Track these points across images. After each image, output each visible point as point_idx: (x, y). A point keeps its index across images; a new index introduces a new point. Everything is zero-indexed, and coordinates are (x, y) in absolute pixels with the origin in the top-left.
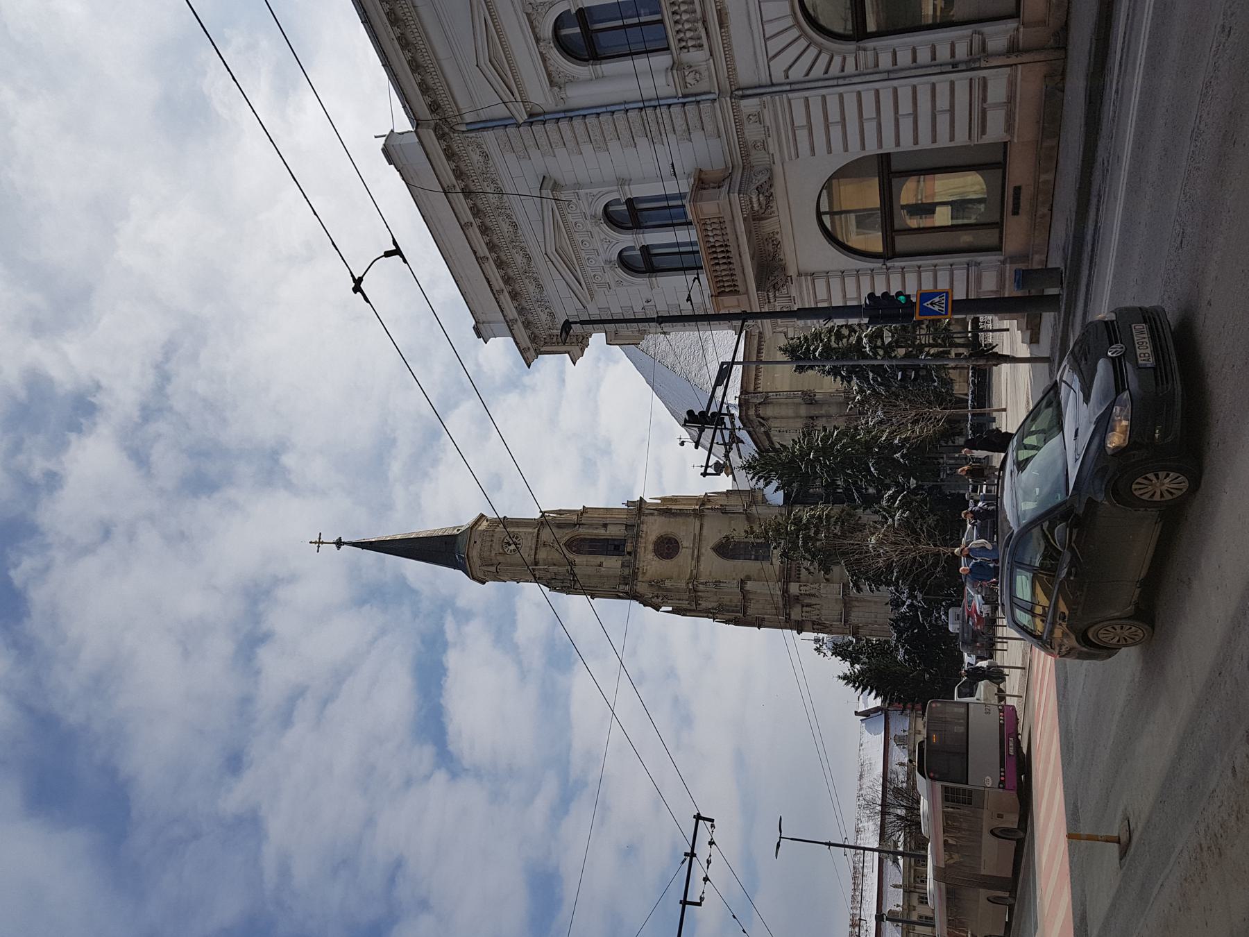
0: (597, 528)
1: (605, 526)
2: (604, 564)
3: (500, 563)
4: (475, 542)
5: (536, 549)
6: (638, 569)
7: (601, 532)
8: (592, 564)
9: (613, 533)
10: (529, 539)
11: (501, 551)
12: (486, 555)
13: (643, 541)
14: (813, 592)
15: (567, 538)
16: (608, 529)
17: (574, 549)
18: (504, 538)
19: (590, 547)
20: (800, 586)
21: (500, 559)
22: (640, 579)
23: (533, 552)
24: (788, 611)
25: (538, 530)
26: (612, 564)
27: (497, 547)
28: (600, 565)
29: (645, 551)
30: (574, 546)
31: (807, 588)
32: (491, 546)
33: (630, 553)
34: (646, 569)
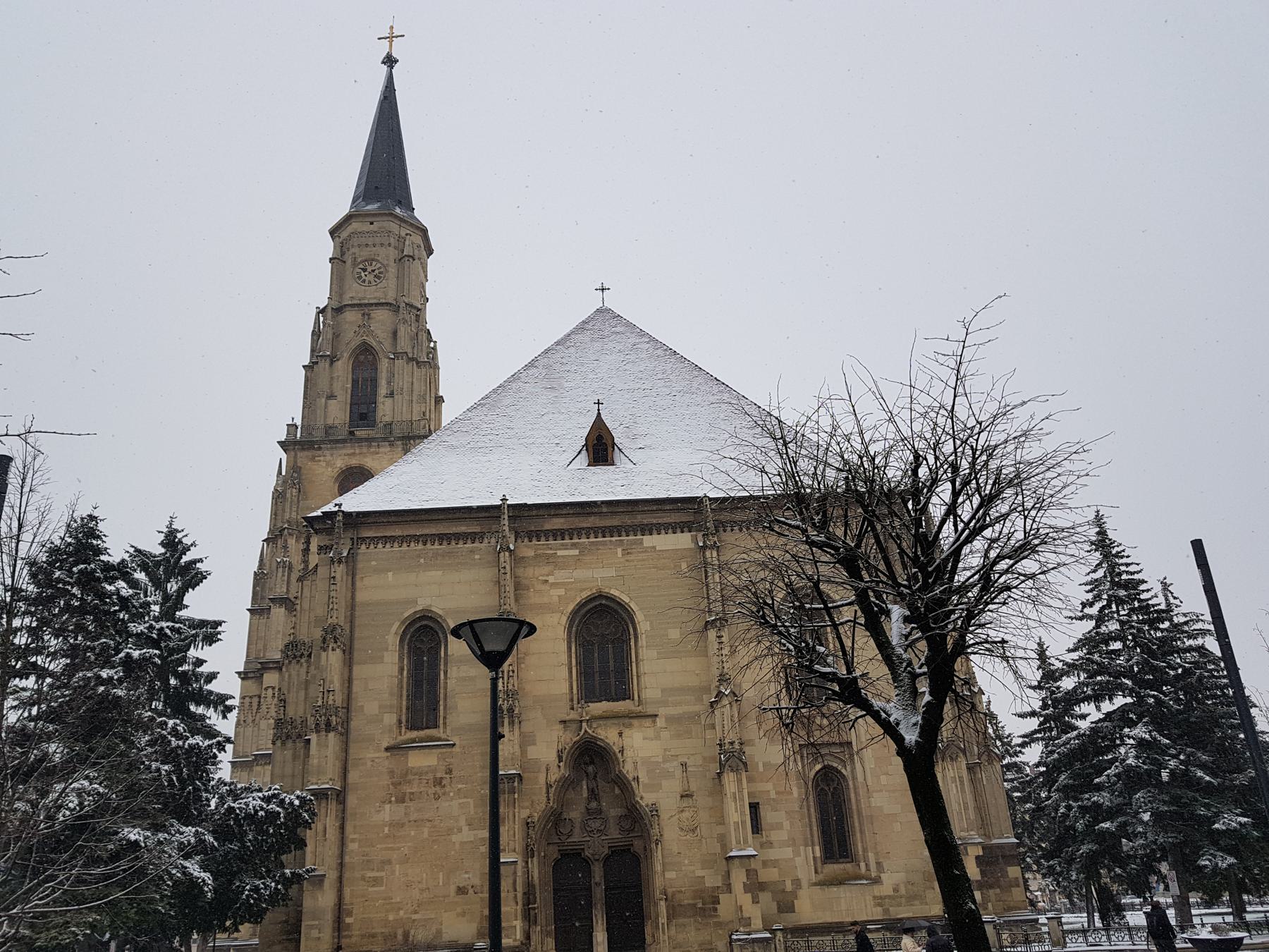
0: (389, 383)
1: (391, 395)
2: (330, 402)
3: (345, 262)
4: (372, 223)
5: (360, 305)
6: (320, 448)
7: (383, 390)
8: (335, 385)
9: (380, 406)
10: (377, 295)
11: (359, 260)
12: (355, 241)
13: (365, 450)
14: (264, 707)
15: (374, 344)
16: (387, 399)
17: (362, 358)
18: (377, 261)
19: (365, 380)
20: (273, 688)
21: (349, 262)
22: (300, 454)
23: (355, 302)
24: (250, 675)
25: (391, 304)
26: (338, 413)
27: (365, 253)
28: (331, 396)
29: (348, 455)
30: (366, 358)
31: (270, 699)
32: (367, 245)
33: (352, 433)
34: (320, 461)
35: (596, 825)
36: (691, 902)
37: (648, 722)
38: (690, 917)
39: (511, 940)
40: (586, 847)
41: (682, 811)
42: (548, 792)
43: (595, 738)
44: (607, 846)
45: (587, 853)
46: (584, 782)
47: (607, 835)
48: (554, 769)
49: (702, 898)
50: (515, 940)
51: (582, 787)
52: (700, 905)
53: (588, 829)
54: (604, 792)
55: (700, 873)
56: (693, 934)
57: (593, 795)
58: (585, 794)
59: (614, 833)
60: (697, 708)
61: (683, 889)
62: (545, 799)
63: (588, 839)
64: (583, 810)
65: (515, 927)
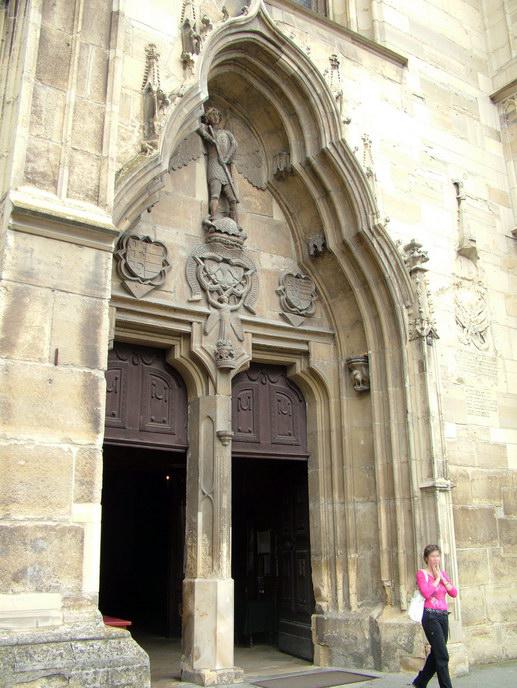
35: (225, 276)
36: (485, 504)
37: (390, 68)
38: (483, 543)
39: (50, 602)
40: (196, 331)
41: (458, 285)
42: (150, 114)
43: (281, 41)
44: (250, 340)
45: (196, 347)
46: (200, 167)
47: (252, 313)
48: (176, 67)
49: (503, 496)
50: (73, 601)
51: (193, 175)
52: (500, 514)
53: (208, 285)
54: (248, 205)
55: (499, 436)
56: (490, 587)
57: (224, 199)
58: (202, 195)
59: (268, 312)
60: (470, 91)
61: (470, 470)
62: (136, 136)
63: (203, 308)
64: (195, 229)
65: (78, 533)
